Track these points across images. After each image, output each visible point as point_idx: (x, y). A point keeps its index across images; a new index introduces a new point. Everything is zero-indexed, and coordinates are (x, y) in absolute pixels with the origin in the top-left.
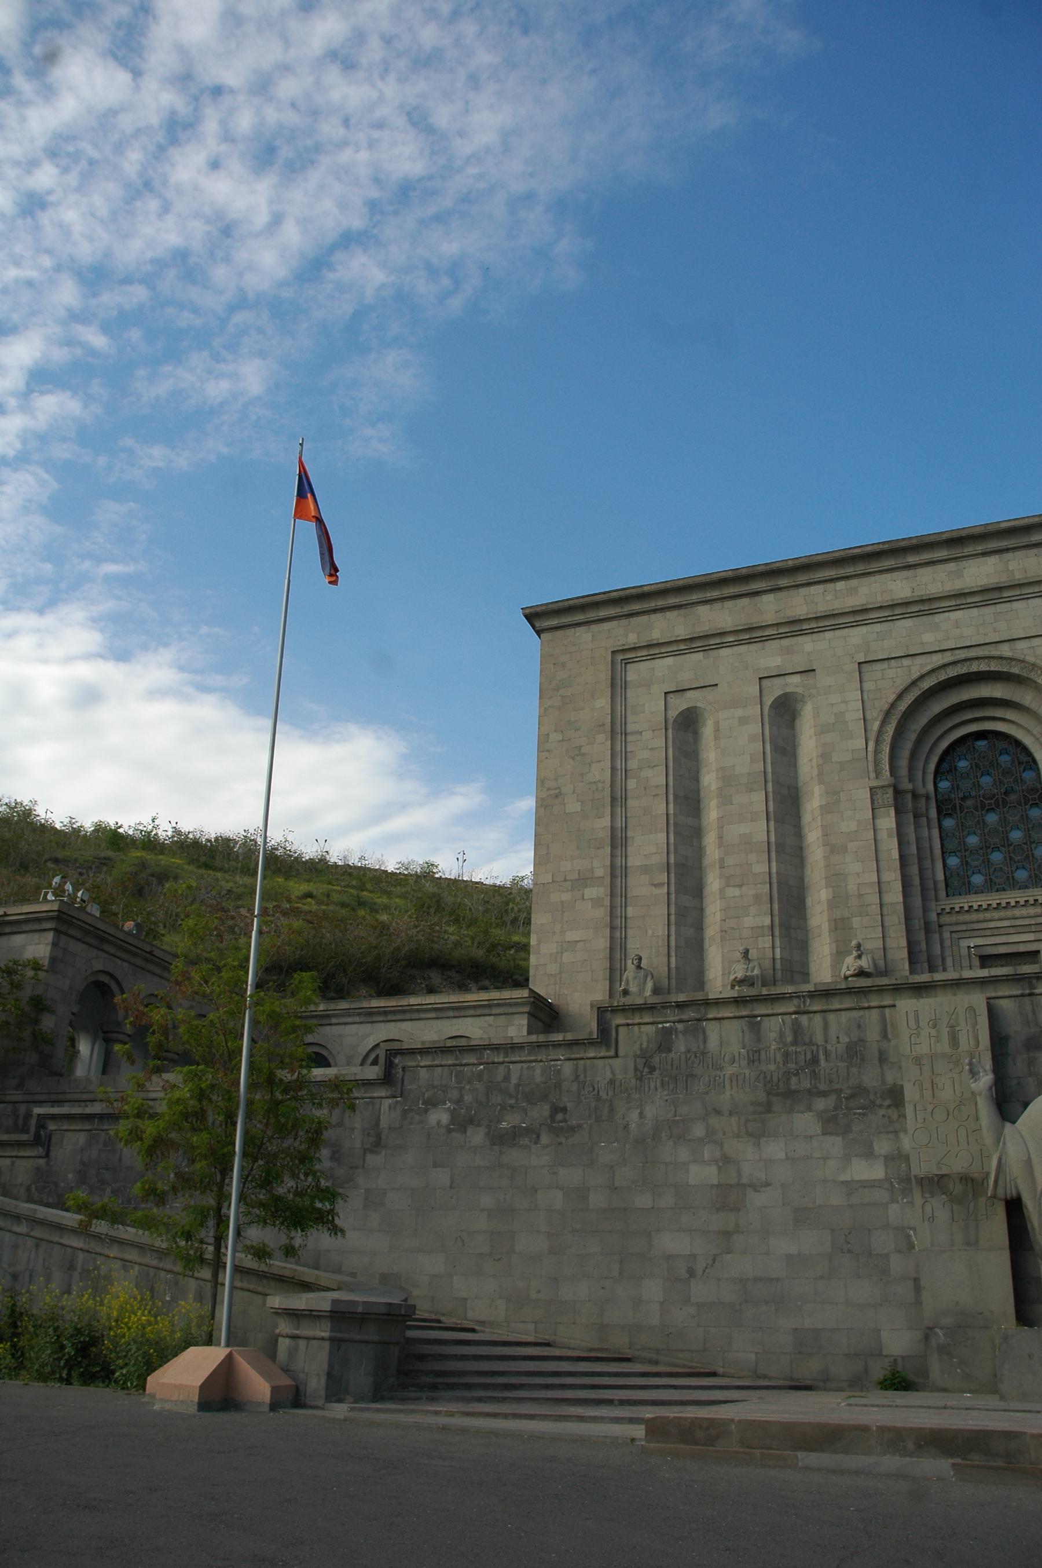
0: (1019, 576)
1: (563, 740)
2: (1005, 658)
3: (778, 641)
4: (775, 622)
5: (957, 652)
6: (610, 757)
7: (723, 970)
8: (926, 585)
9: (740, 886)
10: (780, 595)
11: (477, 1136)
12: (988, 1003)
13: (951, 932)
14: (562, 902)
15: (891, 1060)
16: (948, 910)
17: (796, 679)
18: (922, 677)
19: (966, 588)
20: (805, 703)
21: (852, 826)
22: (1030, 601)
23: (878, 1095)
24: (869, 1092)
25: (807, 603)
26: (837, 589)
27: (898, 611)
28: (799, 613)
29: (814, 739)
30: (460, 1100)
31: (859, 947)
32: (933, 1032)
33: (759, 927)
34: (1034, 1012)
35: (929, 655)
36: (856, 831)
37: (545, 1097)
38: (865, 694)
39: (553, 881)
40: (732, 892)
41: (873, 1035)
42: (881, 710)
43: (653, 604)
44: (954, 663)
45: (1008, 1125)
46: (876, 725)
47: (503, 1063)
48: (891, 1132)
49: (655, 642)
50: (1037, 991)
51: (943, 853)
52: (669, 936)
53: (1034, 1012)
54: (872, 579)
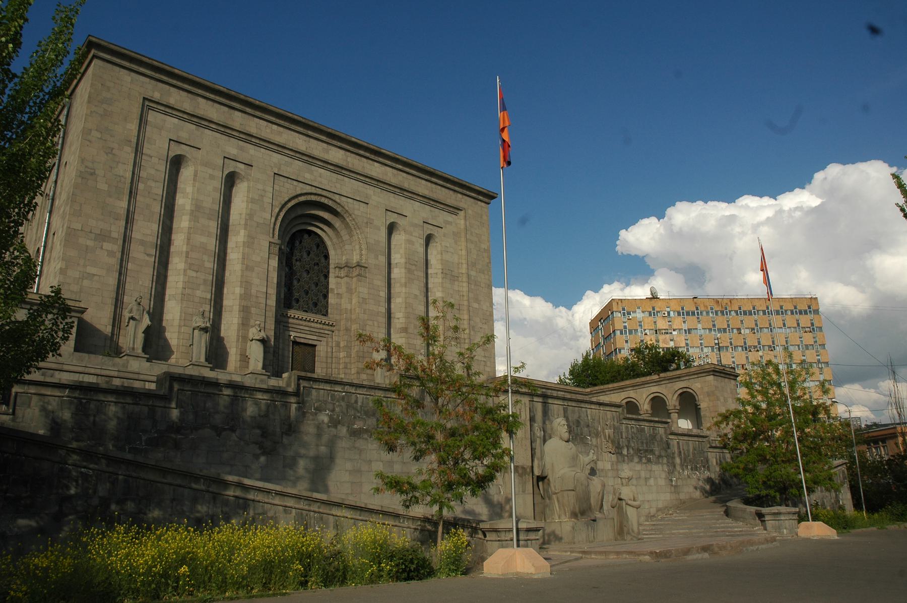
0: (350, 166)
1: (101, 138)
5: (317, 189)
6: (132, 164)
7: (181, 316)
9: (197, 272)
10: (243, 115)
11: (343, 431)
14: (87, 246)
17: (242, 166)
20: (242, 181)
21: (259, 259)
27: (298, 155)
30: (333, 410)
33: (203, 298)
36: (260, 262)
37: (374, 415)
39: (82, 230)
40: (192, 273)
43: (174, 82)
44: (315, 194)
46: (277, 210)
47: (354, 393)
49: (172, 106)
50: (535, 400)
52: (152, 288)
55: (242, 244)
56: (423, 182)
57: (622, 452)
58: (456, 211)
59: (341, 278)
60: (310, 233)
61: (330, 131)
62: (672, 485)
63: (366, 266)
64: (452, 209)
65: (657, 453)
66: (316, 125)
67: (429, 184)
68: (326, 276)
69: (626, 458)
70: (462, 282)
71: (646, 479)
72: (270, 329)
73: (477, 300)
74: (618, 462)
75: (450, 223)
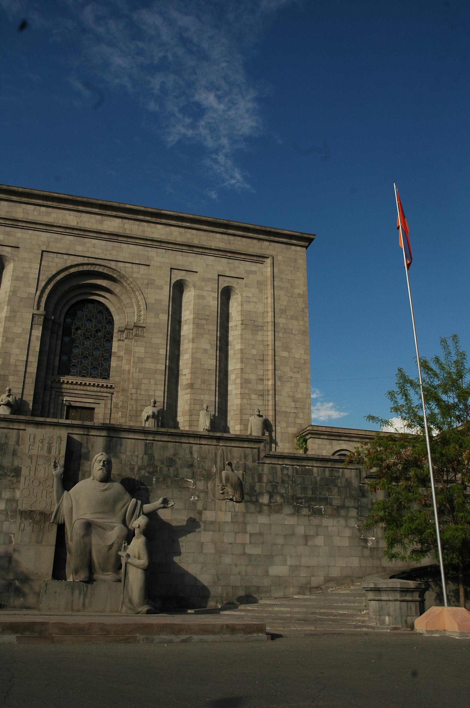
0: (128, 232)
2: (112, 269)
3: (4, 227)
4: (5, 217)
5: (91, 259)
8: (84, 222)
12: (68, 435)
13: (56, 392)
15: (19, 454)
16: (57, 381)
17: (9, 249)
18: (71, 267)
19: (103, 230)
21: (20, 330)
22: (130, 245)
23: (9, 470)
24: (5, 468)
25: (23, 212)
26: (41, 210)
27: (68, 231)
28: (18, 216)
29: (10, 282)
31: (10, 390)
32: (41, 445)
34: (87, 443)
35: (77, 257)
38: (42, 267)
41: (12, 442)
42: (47, 277)
44: (88, 264)
45: (66, 492)
46: (42, 284)
48: (12, 488)
50: (90, 434)
51: (61, 353)
53: (87, 443)
54: (60, 211)
55: (3, 319)
56: (218, 236)
57: (257, 501)
58: (261, 259)
59: (123, 341)
60: (93, 301)
61: (100, 202)
62: (366, 547)
63: (144, 325)
64: (255, 258)
65: (336, 502)
66: (85, 200)
67: (226, 237)
68: (110, 340)
69: (265, 508)
70: (267, 331)
71: (306, 537)
72: (29, 395)
73: (286, 348)
74: (247, 511)
75: (255, 273)
